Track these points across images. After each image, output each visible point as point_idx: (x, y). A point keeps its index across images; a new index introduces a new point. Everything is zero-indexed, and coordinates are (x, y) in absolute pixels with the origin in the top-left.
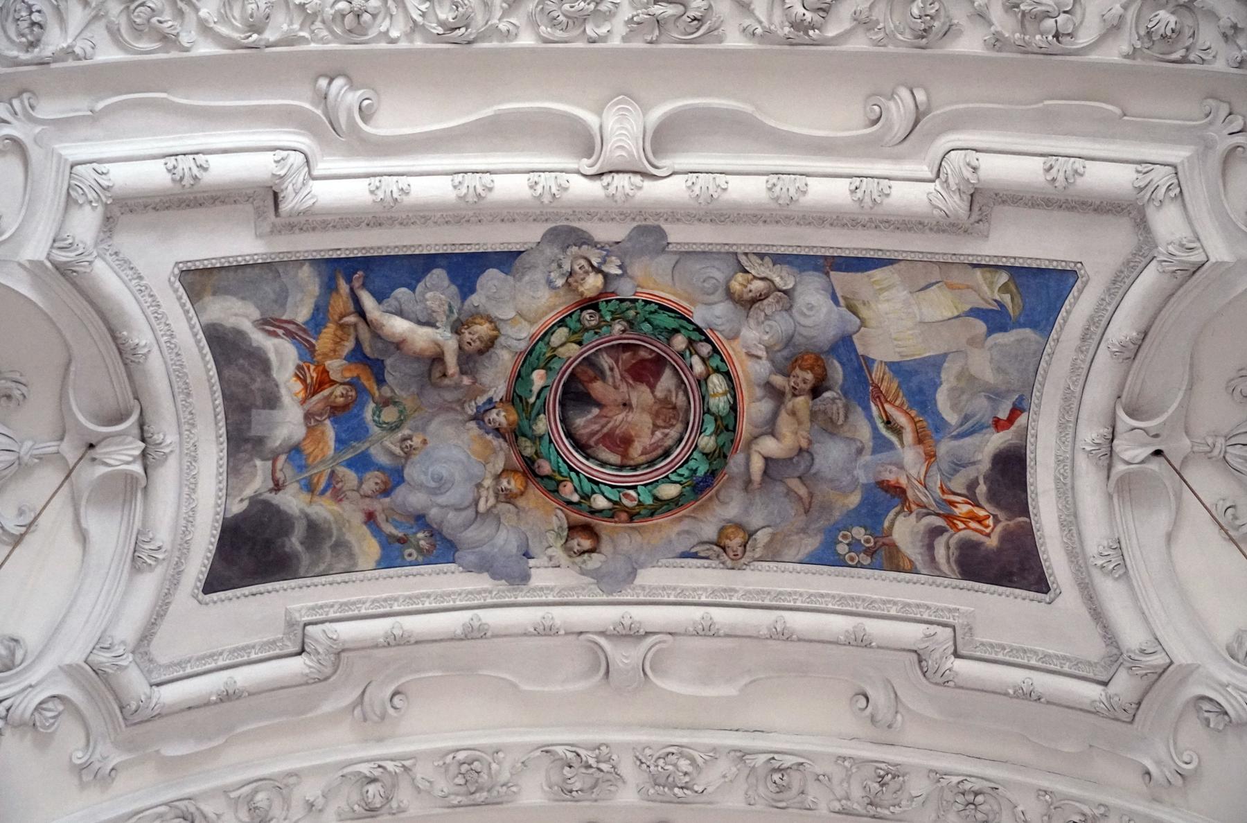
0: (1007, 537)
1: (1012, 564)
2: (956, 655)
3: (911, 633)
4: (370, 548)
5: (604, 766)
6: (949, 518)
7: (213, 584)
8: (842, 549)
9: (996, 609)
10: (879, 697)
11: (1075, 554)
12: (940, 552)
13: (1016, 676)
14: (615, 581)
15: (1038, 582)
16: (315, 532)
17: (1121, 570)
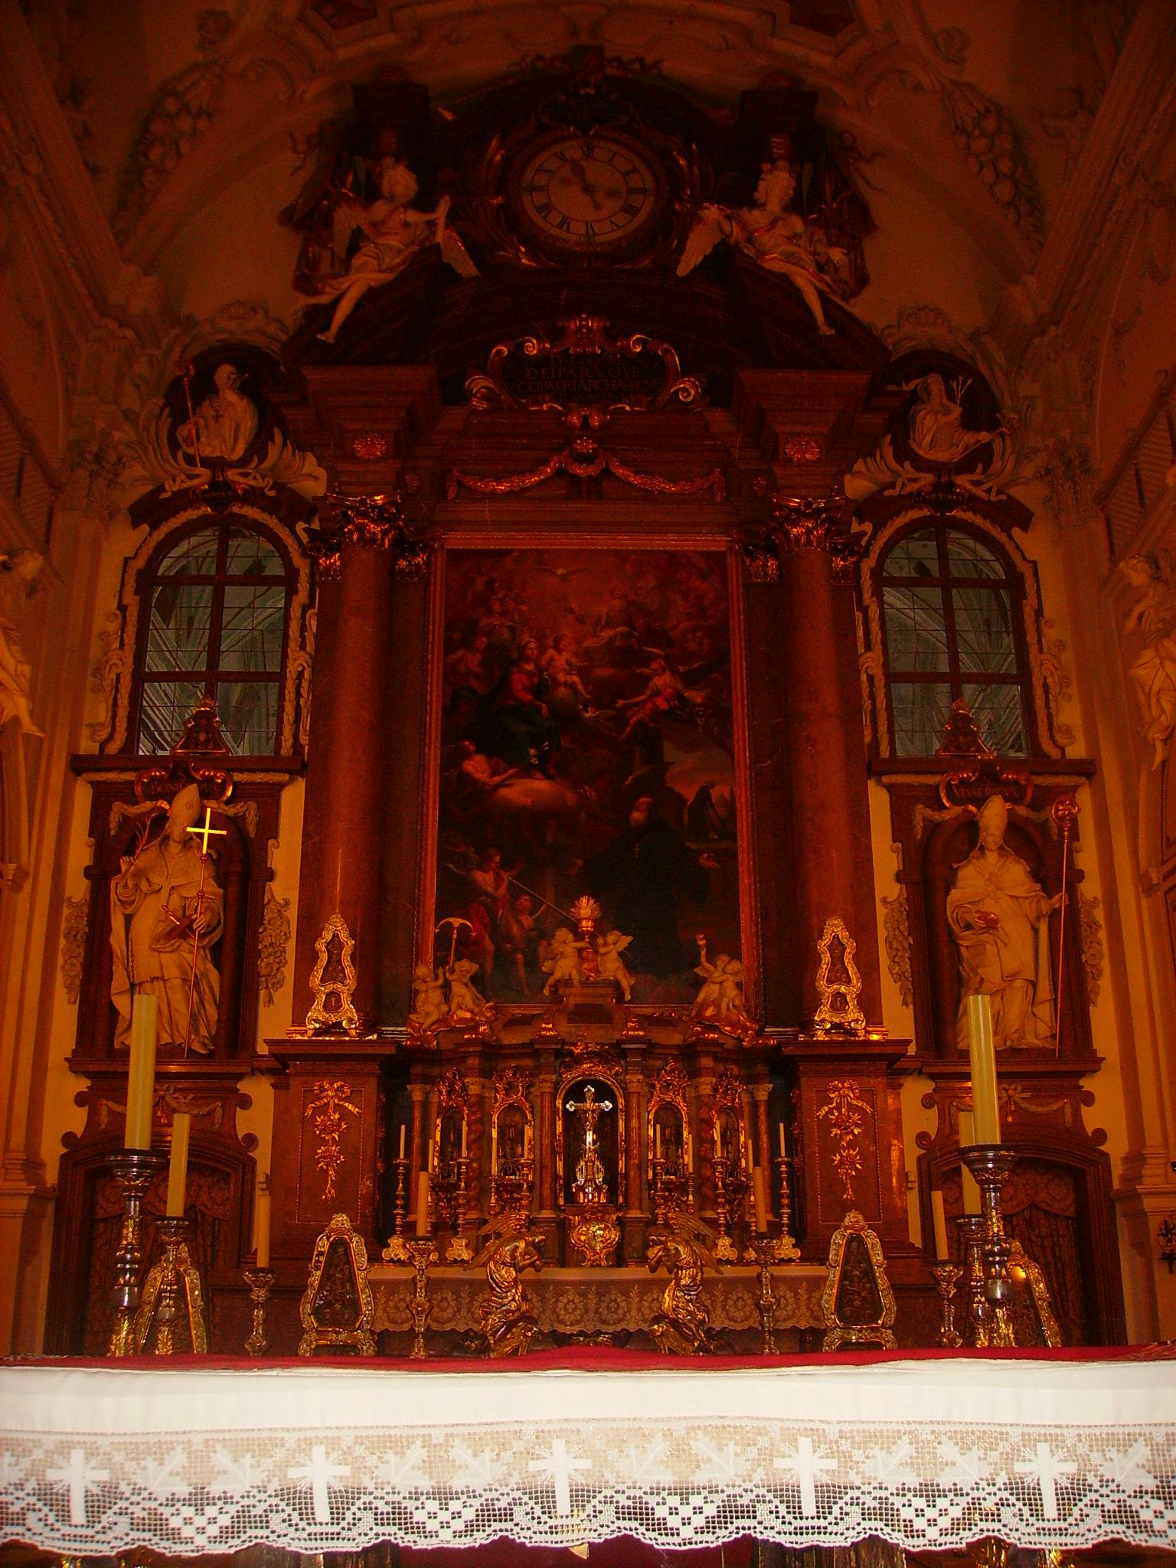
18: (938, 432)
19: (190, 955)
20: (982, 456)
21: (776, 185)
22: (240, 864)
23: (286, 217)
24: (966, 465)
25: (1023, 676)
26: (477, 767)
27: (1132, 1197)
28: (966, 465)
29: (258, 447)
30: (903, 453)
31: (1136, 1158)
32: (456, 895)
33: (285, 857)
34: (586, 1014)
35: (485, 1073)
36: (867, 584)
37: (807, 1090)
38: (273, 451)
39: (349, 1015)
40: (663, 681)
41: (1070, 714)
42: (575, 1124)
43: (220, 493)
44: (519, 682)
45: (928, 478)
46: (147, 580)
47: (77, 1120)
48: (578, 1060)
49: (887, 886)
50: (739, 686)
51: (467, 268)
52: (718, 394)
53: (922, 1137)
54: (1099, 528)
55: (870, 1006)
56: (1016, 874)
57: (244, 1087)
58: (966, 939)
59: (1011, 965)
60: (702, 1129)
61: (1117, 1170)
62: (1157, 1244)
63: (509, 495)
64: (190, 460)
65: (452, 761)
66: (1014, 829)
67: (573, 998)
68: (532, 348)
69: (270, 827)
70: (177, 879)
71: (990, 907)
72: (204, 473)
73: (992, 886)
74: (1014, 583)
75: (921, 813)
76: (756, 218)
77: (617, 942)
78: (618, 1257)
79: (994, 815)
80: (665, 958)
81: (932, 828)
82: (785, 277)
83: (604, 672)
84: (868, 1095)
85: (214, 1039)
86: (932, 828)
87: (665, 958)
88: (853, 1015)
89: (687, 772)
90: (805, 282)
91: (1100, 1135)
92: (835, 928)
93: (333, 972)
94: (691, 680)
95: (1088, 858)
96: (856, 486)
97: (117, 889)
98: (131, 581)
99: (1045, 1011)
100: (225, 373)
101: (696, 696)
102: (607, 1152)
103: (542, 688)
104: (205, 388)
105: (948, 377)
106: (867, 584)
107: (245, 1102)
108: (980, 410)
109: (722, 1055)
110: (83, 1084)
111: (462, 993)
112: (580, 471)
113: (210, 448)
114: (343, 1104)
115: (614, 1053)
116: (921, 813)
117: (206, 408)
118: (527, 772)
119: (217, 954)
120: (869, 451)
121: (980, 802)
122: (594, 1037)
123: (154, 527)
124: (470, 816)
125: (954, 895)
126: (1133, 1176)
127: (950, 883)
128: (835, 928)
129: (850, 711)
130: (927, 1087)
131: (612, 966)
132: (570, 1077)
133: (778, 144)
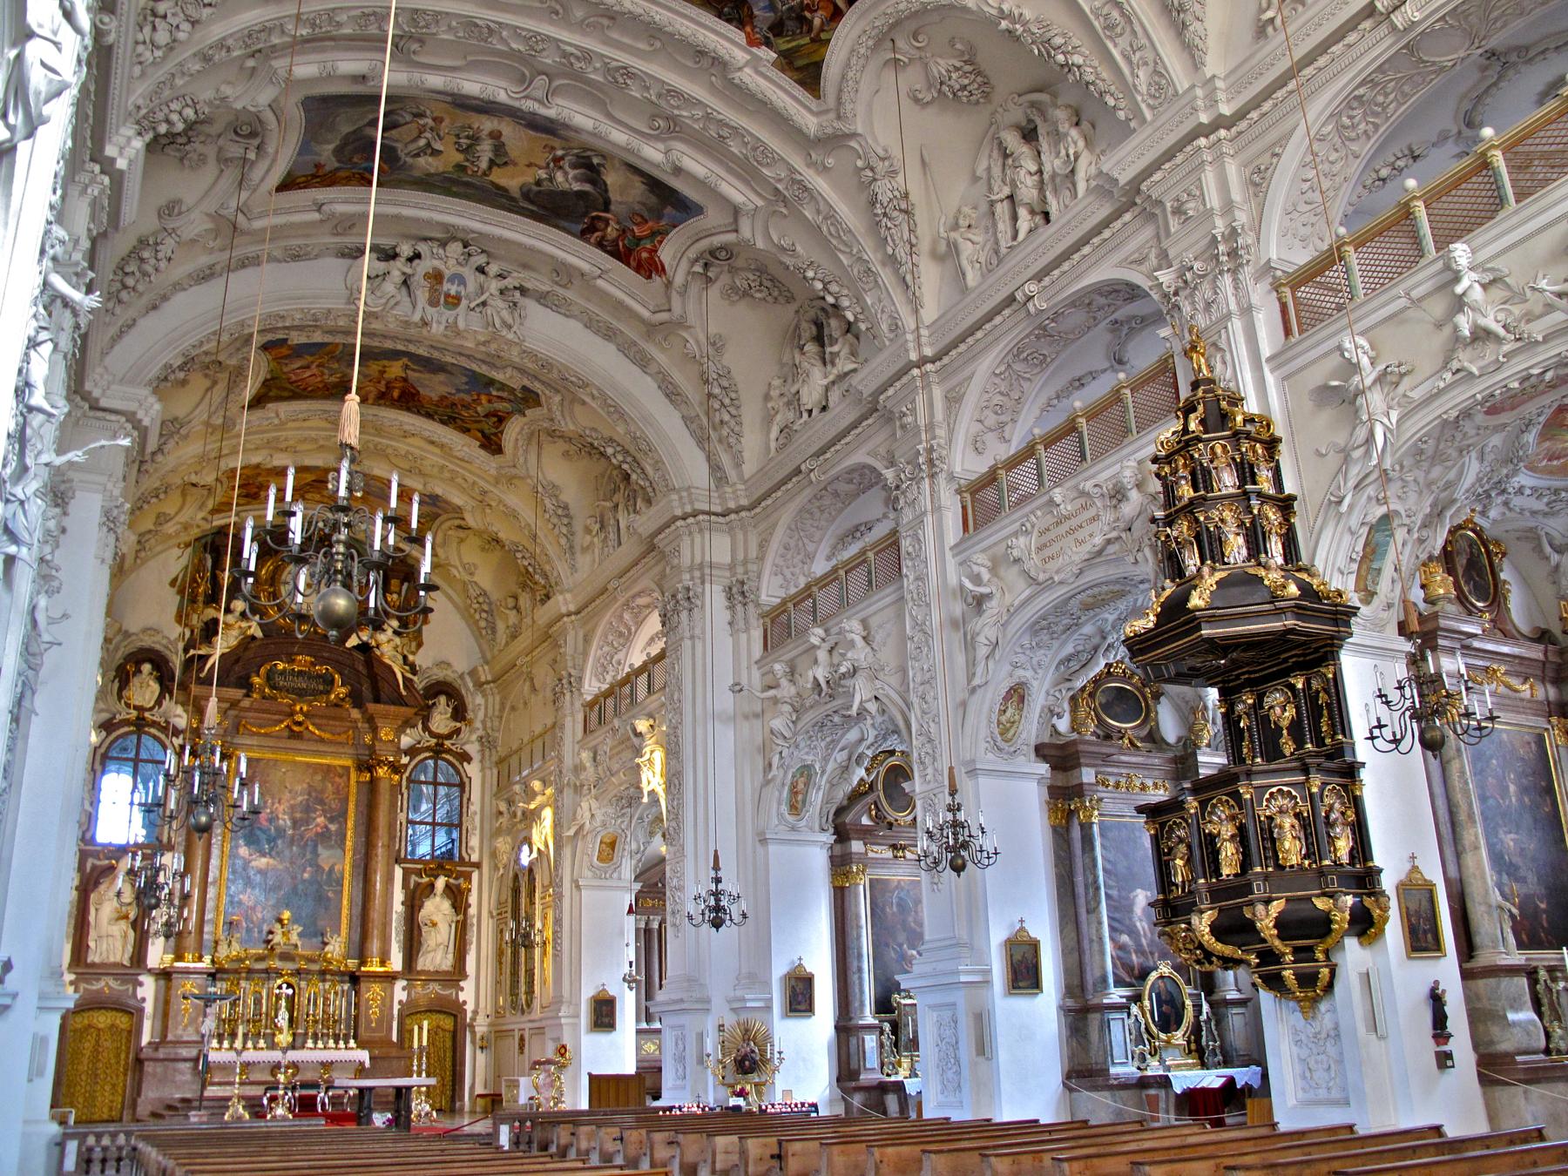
18: (441, 720)
19: (124, 925)
20: (458, 731)
23: (173, 583)
24: (449, 737)
25: (460, 825)
26: (243, 851)
27: (472, 1027)
28: (449, 737)
29: (159, 702)
30: (426, 728)
31: (475, 1012)
34: (285, 957)
35: (247, 979)
36: (404, 783)
37: (363, 986)
38: (166, 703)
40: (321, 820)
41: (474, 841)
42: (278, 997)
43: (140, 724)
45: (434, 741)
48: (282, 976)
49: (398, 906)
50: (350, 824)
51: (259, 634)
52: (356, 699)
53: (400, 1002)
54: (495, 771)
56: (446, 905)
57: (141, 978)
58: (424, 929)
59: (440, 940)
60: (326, 999)
61: (469, 1015)
62: (479, 1043)
63: (266, 735)
64: (128, 705)
66: (447, 886)
67: (278, 951)
68: (281, 666)
71: (435, 919)
72: (134, 713)
73: (437, 909)
74: (462, 786)
75: (414, 878)
76: (382, 637)
77: (298, 929)
78: (293, 1047)
79: (441, 883)
81: (417, 885)
82: (390, 667)
83: (298, 815)
84: (384, 990)
85: (131, 959)
86: (417, 885)
87: (316, 934)
89: (326, 856)
90: (397, 670)
91: (465, 1003)
94: (331, 820)
95: (473, 899)
96: (406, 741)
98: (98, 757)
99: (450, 956)
100: (147, 667)
101: (333, 827)
102: (291, 1010)
103: (273, 819)
105: (449, 696)
106: (404, 783)
107: (141, 984)
108: (459, 713)
109: (333, 973)
110: (73, 977)
112: (296, 728)
113: (137, 700)
115: (298, 973)
116: (414, 878)
117: (135, 681)
118: (264, 855)
119: (134, 925)
120: (414, 726)
121: (436, 877)
122: (289, 966)
123: (108, 734)
125: (423, 913)
126: (473, 1019)
127: (421, 907)
129: (392, 837)
130: (404, 983)
131: (294, 938)
132: (279, 982)
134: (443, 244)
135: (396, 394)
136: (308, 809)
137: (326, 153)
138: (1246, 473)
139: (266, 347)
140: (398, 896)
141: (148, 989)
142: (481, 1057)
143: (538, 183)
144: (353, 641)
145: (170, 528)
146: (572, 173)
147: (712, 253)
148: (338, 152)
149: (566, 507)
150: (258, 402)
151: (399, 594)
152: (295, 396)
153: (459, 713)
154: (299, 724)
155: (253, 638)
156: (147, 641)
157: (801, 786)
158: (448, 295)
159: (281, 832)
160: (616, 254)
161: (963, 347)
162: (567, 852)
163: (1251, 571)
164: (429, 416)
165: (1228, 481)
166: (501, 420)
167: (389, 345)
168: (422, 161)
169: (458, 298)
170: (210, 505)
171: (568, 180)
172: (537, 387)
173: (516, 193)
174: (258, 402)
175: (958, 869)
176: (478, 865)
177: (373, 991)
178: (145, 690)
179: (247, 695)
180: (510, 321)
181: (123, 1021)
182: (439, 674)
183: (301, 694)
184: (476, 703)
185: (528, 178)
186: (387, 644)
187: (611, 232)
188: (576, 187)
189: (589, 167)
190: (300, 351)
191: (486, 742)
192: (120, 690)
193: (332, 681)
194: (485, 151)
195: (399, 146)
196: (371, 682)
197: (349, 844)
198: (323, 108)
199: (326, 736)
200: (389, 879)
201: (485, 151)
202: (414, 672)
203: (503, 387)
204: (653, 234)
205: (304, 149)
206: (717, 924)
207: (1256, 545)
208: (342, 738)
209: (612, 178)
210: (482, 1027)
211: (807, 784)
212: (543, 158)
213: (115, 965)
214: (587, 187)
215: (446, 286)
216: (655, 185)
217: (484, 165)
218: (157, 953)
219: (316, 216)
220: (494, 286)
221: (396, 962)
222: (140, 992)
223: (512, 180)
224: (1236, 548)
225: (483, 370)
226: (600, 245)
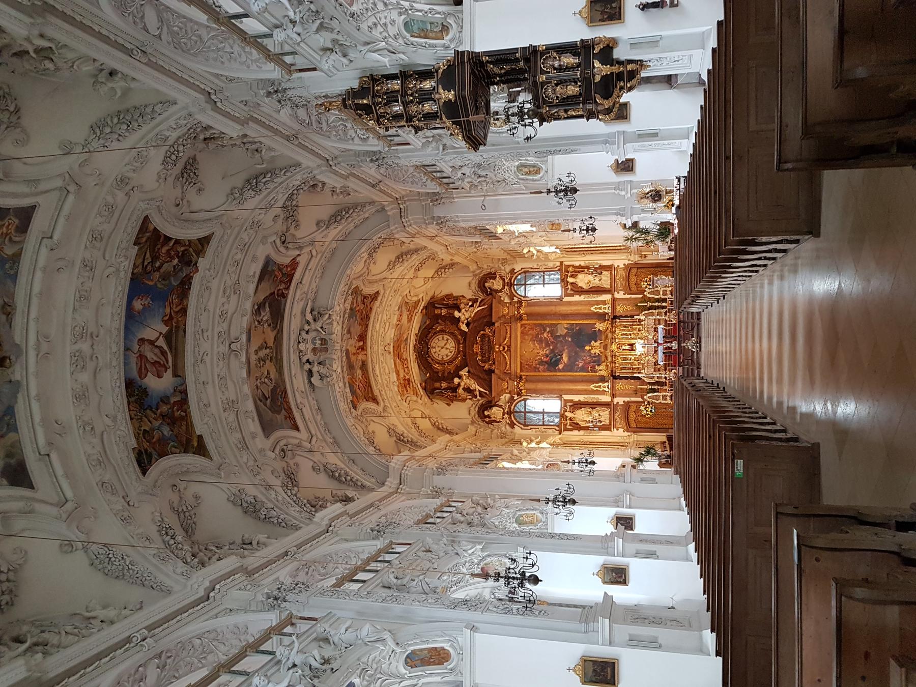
0: (16, 217)
1: (26, 215)
2: (51, 237)
3: (44, 251)
4: (12, 436)
5: (77, 354)
6: (7, 234)
7: (31, 487)
8: (12, 272)
9: (38, 224)
10: (60, 264)
11: (27, 195)
12: (17, 239)
13: (62, 220)
14: (19, 350)
15: (33, 208)
16: (9, 455)
17: (36, 181)
18: (497, 284)
20: (501, 277)
21: (457, 314)
22: (577, 406)
23: (449, 405)
26: (561, 366)
29: (500, 406)
32: (583, 369)
33: (576, 398)
34: (605, 348)
37: (618, 314)
39: (606, 384)
40: (545, 335)
43: (510, 413)
44: (545, 360)
46: (525, 425)
47: (621, 430)
50: (546, 322)
55: (604, 303)
56: (581, 276)
65: (560, 371)
66: (571, 276)
69: (571, 401)
70: (581, 416)
73: (583, 280)
74: (525, 272)
76: (463, 318)
79: (570, 280)
80: (594, 336)
87: (594, 336)
88: (607, 306)
89: (561, 331)
92: (593, 309)
93: (600, 387)
94: (545, 330)
95: (577, 264)
96: (507, 300)
97: (583, 424)
100: (486, 413)
101: (548, 329)
104: (488, 416)
108: (492, 276)
111: (601, 368)
114: (620, 385)
124: (569, 368)
128: (593, 309)
131: (597, 344)
133: (437, 312)
134: (301, 351)
135: (361, 343)
136: (541, 341)
137: (280, 417)
138: (392, 97)
139: (355, 408)
140: (577, 298)
141: (620, 400)
142: (649, 257)
143: (269, 325)
144: (464, 328)
145: (427, 412)
146: (263, 314)
147: (283, 243)
148: (279, 413)
149: (398, 257)
150: (375, 400)
151: (440, 308)
152: (370, 386)
153: (492, 276)
154: (504, 348)
155: (469, 372)
156: (474, 412)
157: (527, 170)
158: (321, 344)
159: (552, 351)
160: (290, 281)
161: (320, 152)
162: (557, 243)
163: (441, 104)
164: (367, 327)
165: (398, 108)
166: (365, 297)
167: (344, 358)
168: (272, 377)
169: (322, 339)
170: (415, 398)
171: (266, 315)
172: (350, 292)
173: (275, 332)
174: (375, 400)
175: (575, 190)
176: (561, 263)
177: (620, 309)
178: (496, 412)
179: (493, 372)
180: (327, 316)
181: (633, 408)
182: (474, 286)
183: (491, 348)
184: (486, 268)
185: (268, 330)
186: (464, 315)
187: (282, 286)
188: (268, 309)
189: (259, 309)
190: (353, 393)
191: (504, 261)
192: (496, 422)
193: (483, 334)
194: (262, 353)
195: (270, 388)
196: (485, 320)
197: (554, 322)
198: (267, 428)
199: (508, 335)
200: (569, 303)
201: (262, 353)
202: (475, 301)
203: (352, 303)
204: (280, 270)
205: (281, 427)
206: (594, 230)
207: (426, 96)
208: (508, 328)
209: (261, 297)
210: (635, 258)
211: (525, 166)
212: (260, 328)
213: (610, 414)
214: (267, 305)
215: (318, 345)
216: (261, 279)
217: (268, 350)
218: (606, 398)
219: (304, 409)
220: (313, 326)
221: (607, 297)
222: (621, 403)
223: (271, 335)
224: (428, 107)
225: (347, 316)
226: (288, 288)
